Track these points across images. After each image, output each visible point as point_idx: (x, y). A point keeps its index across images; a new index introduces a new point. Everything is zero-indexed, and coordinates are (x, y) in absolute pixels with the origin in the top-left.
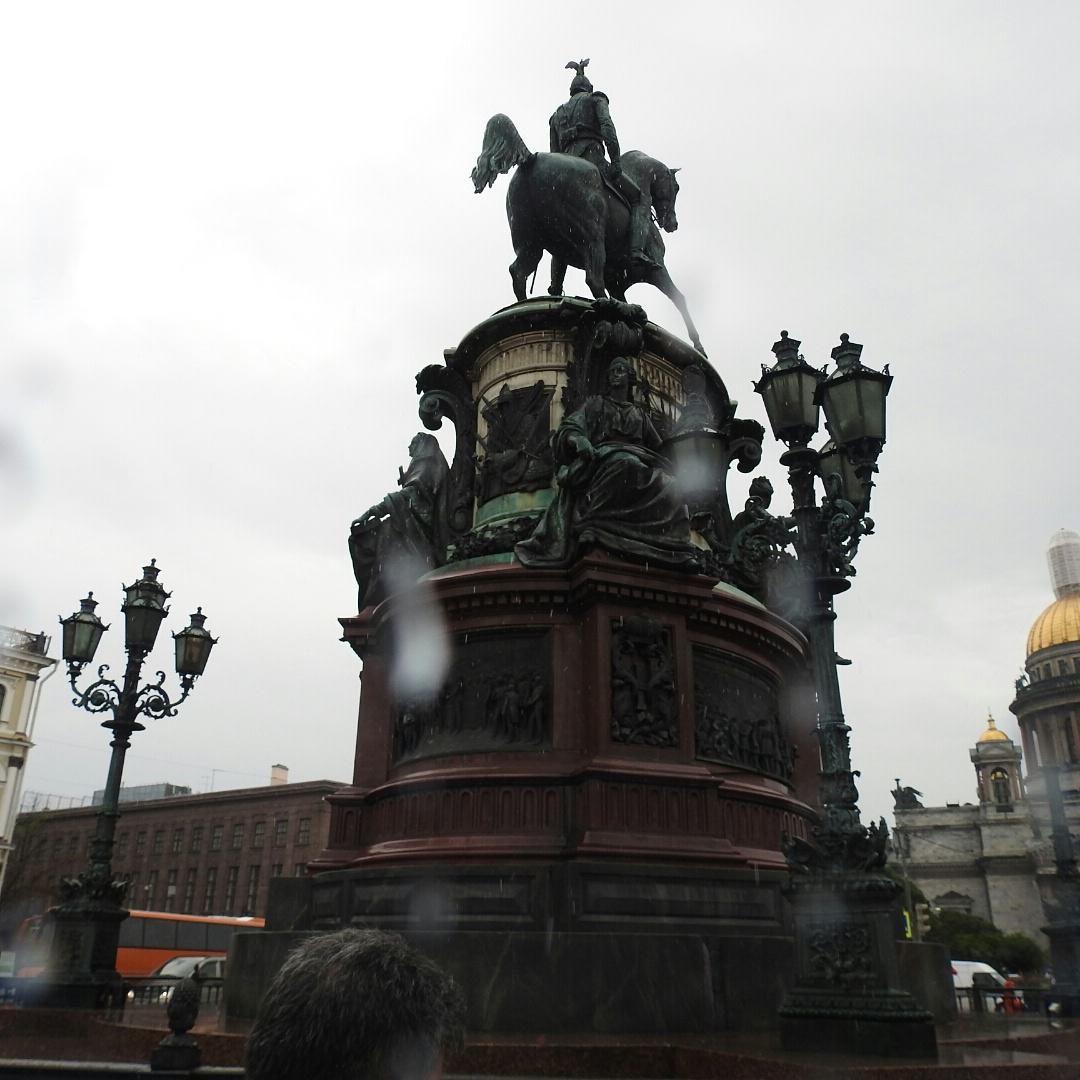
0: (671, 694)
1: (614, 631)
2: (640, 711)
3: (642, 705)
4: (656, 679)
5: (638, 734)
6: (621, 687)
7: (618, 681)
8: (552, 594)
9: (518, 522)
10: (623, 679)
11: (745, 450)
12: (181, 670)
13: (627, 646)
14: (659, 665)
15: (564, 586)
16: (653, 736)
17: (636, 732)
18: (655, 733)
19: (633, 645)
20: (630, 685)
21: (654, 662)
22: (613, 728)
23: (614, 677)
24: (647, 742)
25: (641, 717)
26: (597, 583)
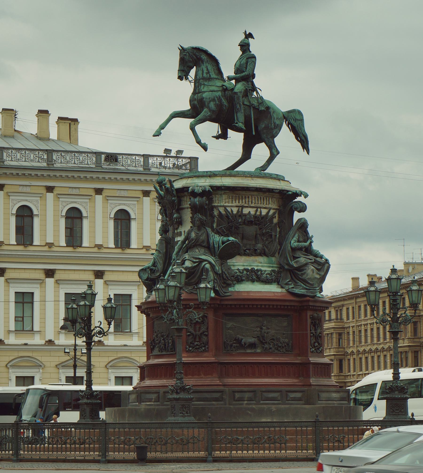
0: (207, 336)
4: (201, 331)
6: (189, 335)
7: (188, 333)
10: (190, 332)
11: (293, 208)
12: (106, 319)
20: (193, 334)
25: (196, 343)
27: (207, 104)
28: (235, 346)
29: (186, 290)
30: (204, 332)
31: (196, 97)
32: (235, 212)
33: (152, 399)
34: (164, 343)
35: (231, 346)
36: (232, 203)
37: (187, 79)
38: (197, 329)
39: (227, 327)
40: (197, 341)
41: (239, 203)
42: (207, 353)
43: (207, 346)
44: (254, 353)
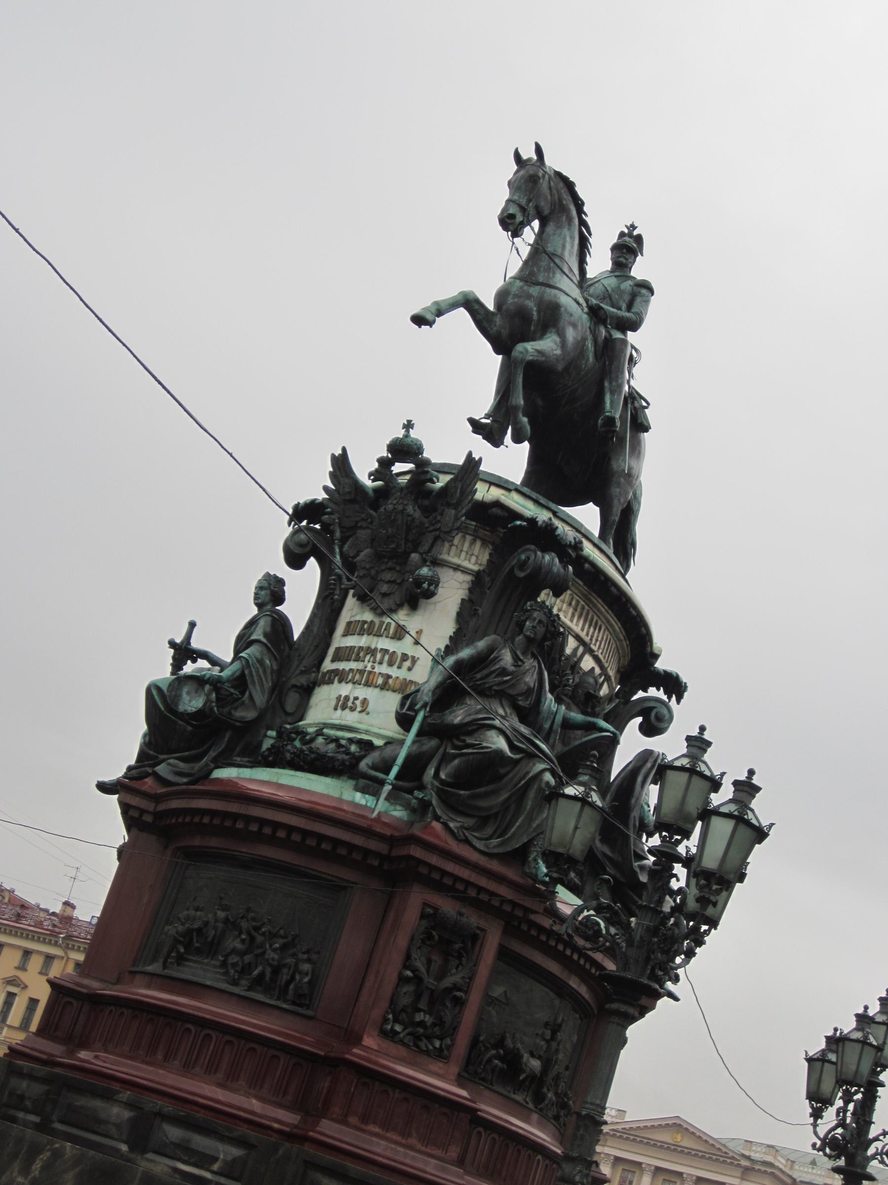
0: (459, 1003)
1: (423, 916)
2: (420, 1010)
3: (422, 1005)
4: (448, 982)
5: (409, 1034)
6: (407, 980)
7: (409, 973)
8: (367, 852)
9: (360, 742)
10: (413, 971)
11: (653, 714)
13: (430, 937)
14: (457, 968)
15: (380, 847)
16: (425, 1041)
17: (407, 1031)
18: (429, 1038)
19: (437, 937)
21: (454, 962)
22: (385, 1020)
23: (406, 967)
24: (418, 1047)
25: (419, 1017)
26: (420, 862)
27: (561, 324)
28: (496, 1066)
29: (452, 825)
30: (456, 987)
31: (535, 291)
32: (568, 651)
33: (215, 1159)
34: (275, 963)
35: (489, 1061)
36: (571, 621)
37: (516, 233)
38: (435, 967)
39: (490, 994)
40: (425, 1012)
41: (582, 630)
42: (441, 1064)
43: (448, 1041)
44: (521, 1105)
